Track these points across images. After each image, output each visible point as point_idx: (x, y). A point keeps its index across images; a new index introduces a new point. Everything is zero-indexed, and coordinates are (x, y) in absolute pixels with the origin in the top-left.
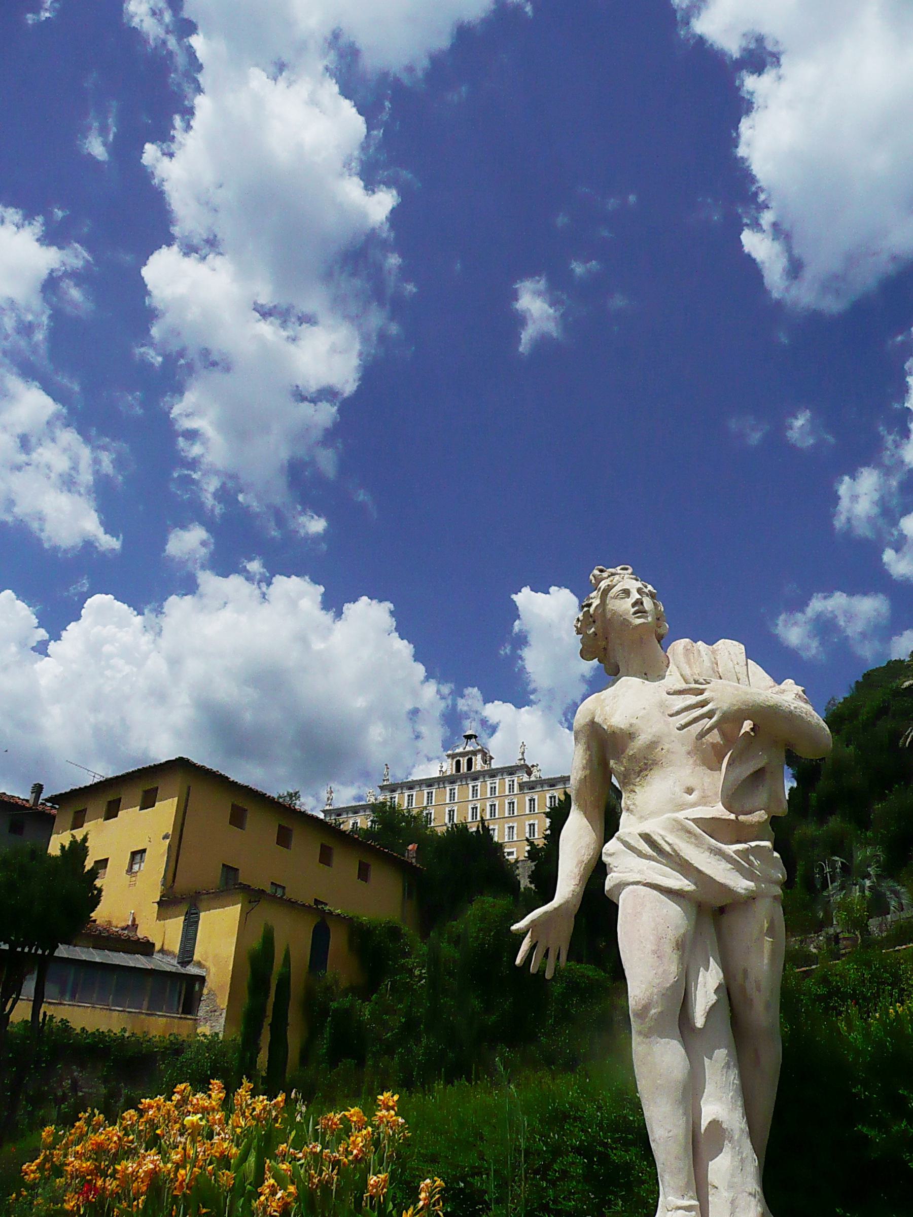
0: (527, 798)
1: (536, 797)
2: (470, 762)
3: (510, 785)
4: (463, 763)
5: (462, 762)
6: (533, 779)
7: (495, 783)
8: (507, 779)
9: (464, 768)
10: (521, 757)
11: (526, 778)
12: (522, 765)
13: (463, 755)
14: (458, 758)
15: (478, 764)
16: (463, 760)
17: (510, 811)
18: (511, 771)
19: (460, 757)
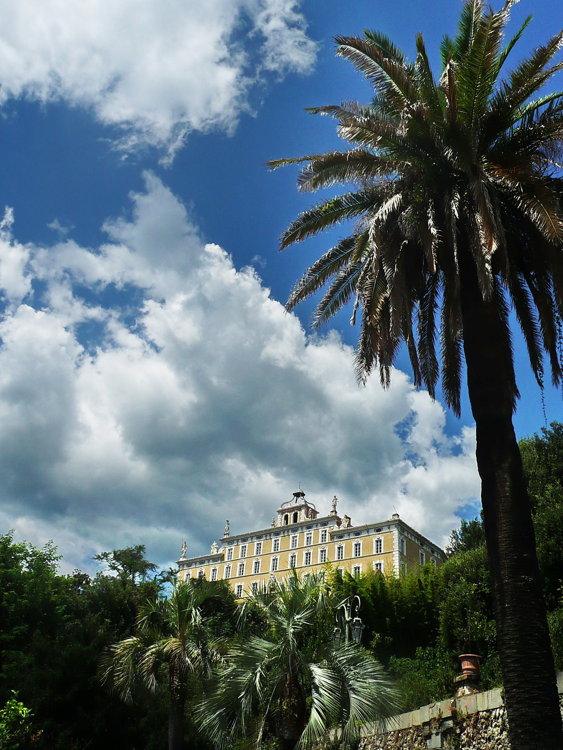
0: (336, 546)
1: (344, 545)
2: (295, 516)
3: (323, 535)
4: (290, 517)
5: (289, 517)
6: (342, 528)
7: (311, 533)
8: (321, 529)
9: (291, 521)
10: (332, 510)
11: (336, 528)
12: (333, 516)
13: (290, 510)
14: (286, 514)
15: (302, 517)
16: (290, 515)
17: (322, 558)
18: (324, 522)
19: (288, 512)
